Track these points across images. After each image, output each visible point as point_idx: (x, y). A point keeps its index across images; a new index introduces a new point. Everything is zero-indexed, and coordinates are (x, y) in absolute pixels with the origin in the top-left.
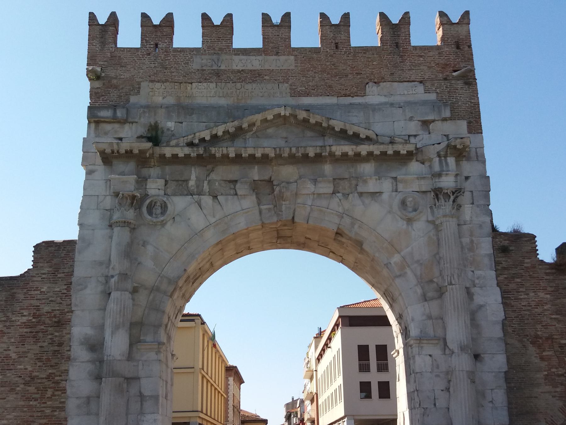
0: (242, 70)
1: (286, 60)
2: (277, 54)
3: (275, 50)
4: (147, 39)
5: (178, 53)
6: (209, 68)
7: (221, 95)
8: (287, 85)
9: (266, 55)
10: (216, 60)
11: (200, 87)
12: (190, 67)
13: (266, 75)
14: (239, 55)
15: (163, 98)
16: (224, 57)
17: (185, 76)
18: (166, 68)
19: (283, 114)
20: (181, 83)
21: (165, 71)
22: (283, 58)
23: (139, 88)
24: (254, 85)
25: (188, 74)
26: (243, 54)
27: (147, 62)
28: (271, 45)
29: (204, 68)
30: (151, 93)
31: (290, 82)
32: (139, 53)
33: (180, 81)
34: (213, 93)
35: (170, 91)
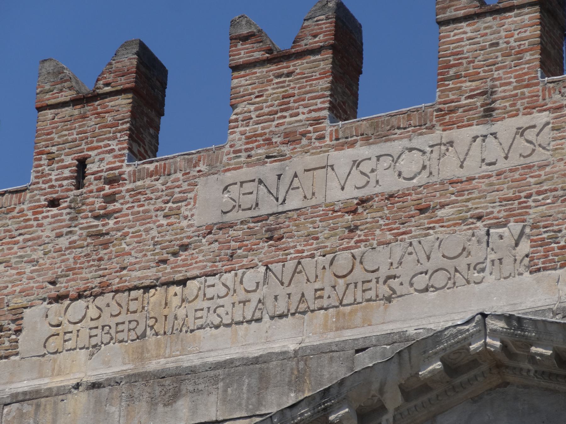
0: (363, 201)
1: (521, 131)
2: (488, 113)
3: (479, 101)
4: (54, 149)
5: (148, 181)
6: (250, 214)
7: (281, 308)
8: (520, 226)
9: (447, 126)
10: (271, 180)
11: (210, 292)
12: (184, 223)
13: (443, 206)
14: (352, 145)
15: (92, 354)
16: (300, 162)
17: (164, 261)
18: (105, 245)
19: (475, 346)
20: (146, 289)
21: (102, 253)
22: (505, 127)
23: (18, 332)
24: (398, 249)
25: (175, 254)
26: (367, 139)
27: (47, 233)
28: (467, 85)
29: (229, 218)
30: (53, 344)
31: (534, 213)
32: (25, 207)
33: (147, 282)
34: (253, 304)
35: (112, 322)
